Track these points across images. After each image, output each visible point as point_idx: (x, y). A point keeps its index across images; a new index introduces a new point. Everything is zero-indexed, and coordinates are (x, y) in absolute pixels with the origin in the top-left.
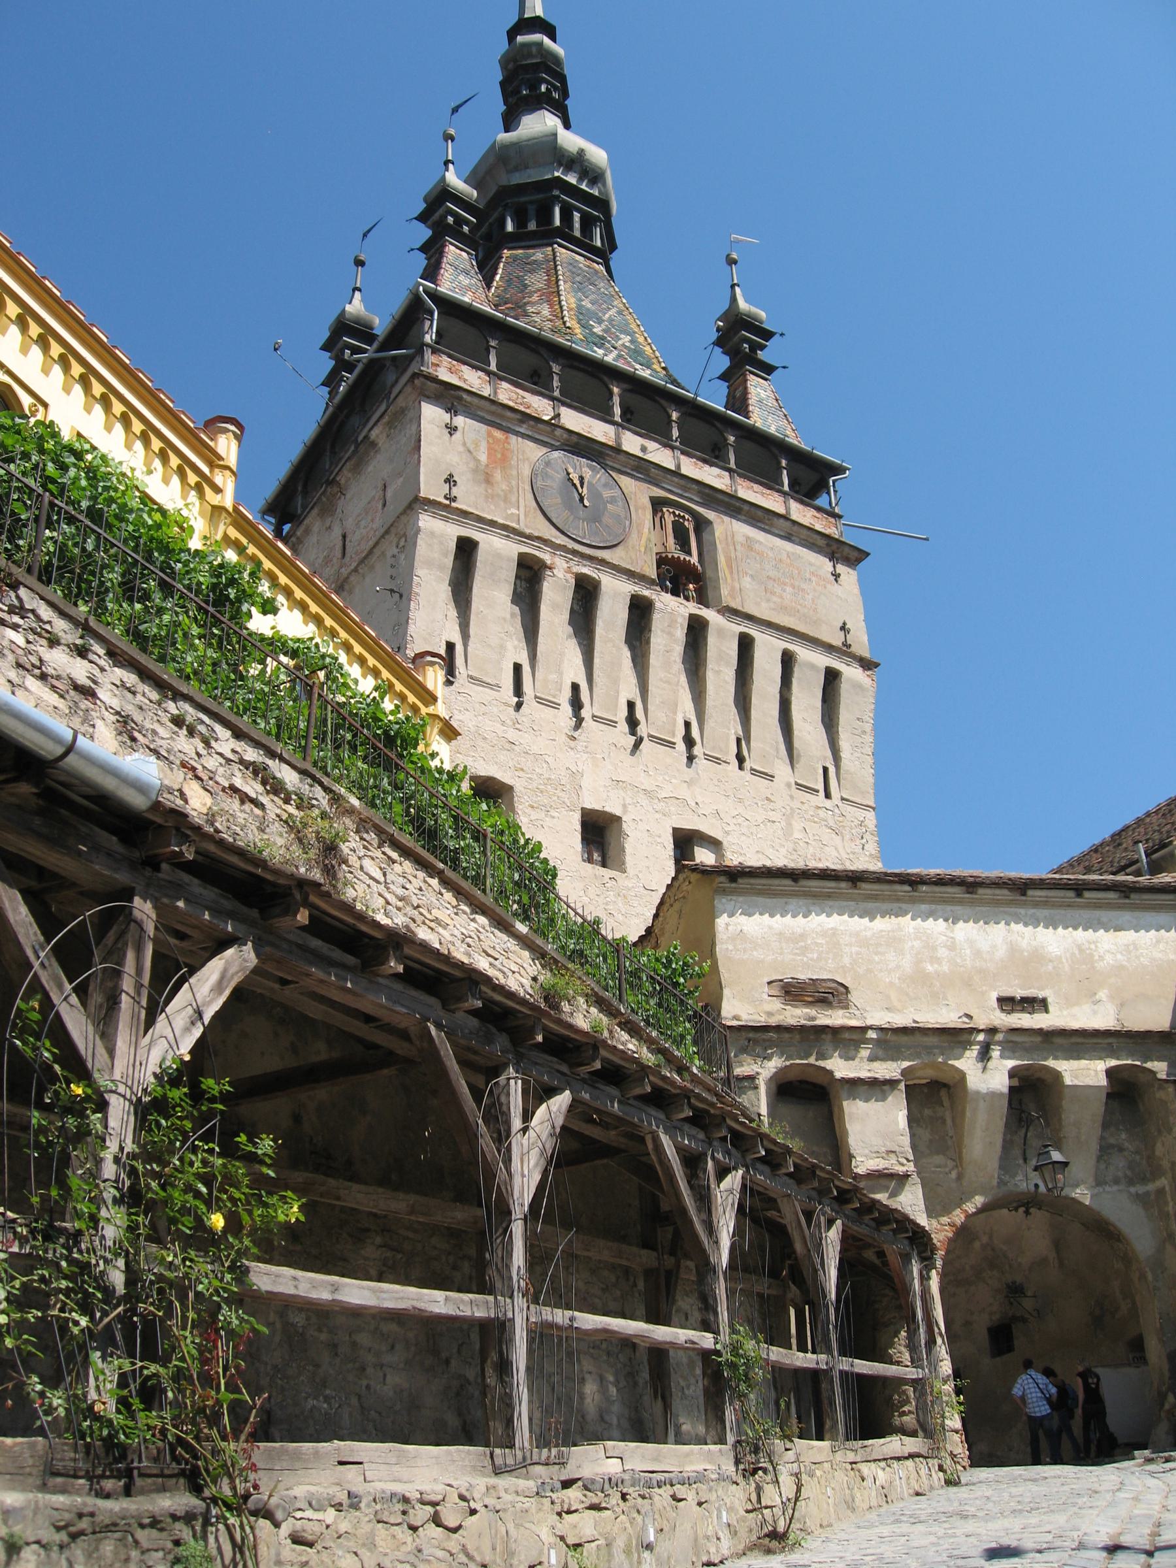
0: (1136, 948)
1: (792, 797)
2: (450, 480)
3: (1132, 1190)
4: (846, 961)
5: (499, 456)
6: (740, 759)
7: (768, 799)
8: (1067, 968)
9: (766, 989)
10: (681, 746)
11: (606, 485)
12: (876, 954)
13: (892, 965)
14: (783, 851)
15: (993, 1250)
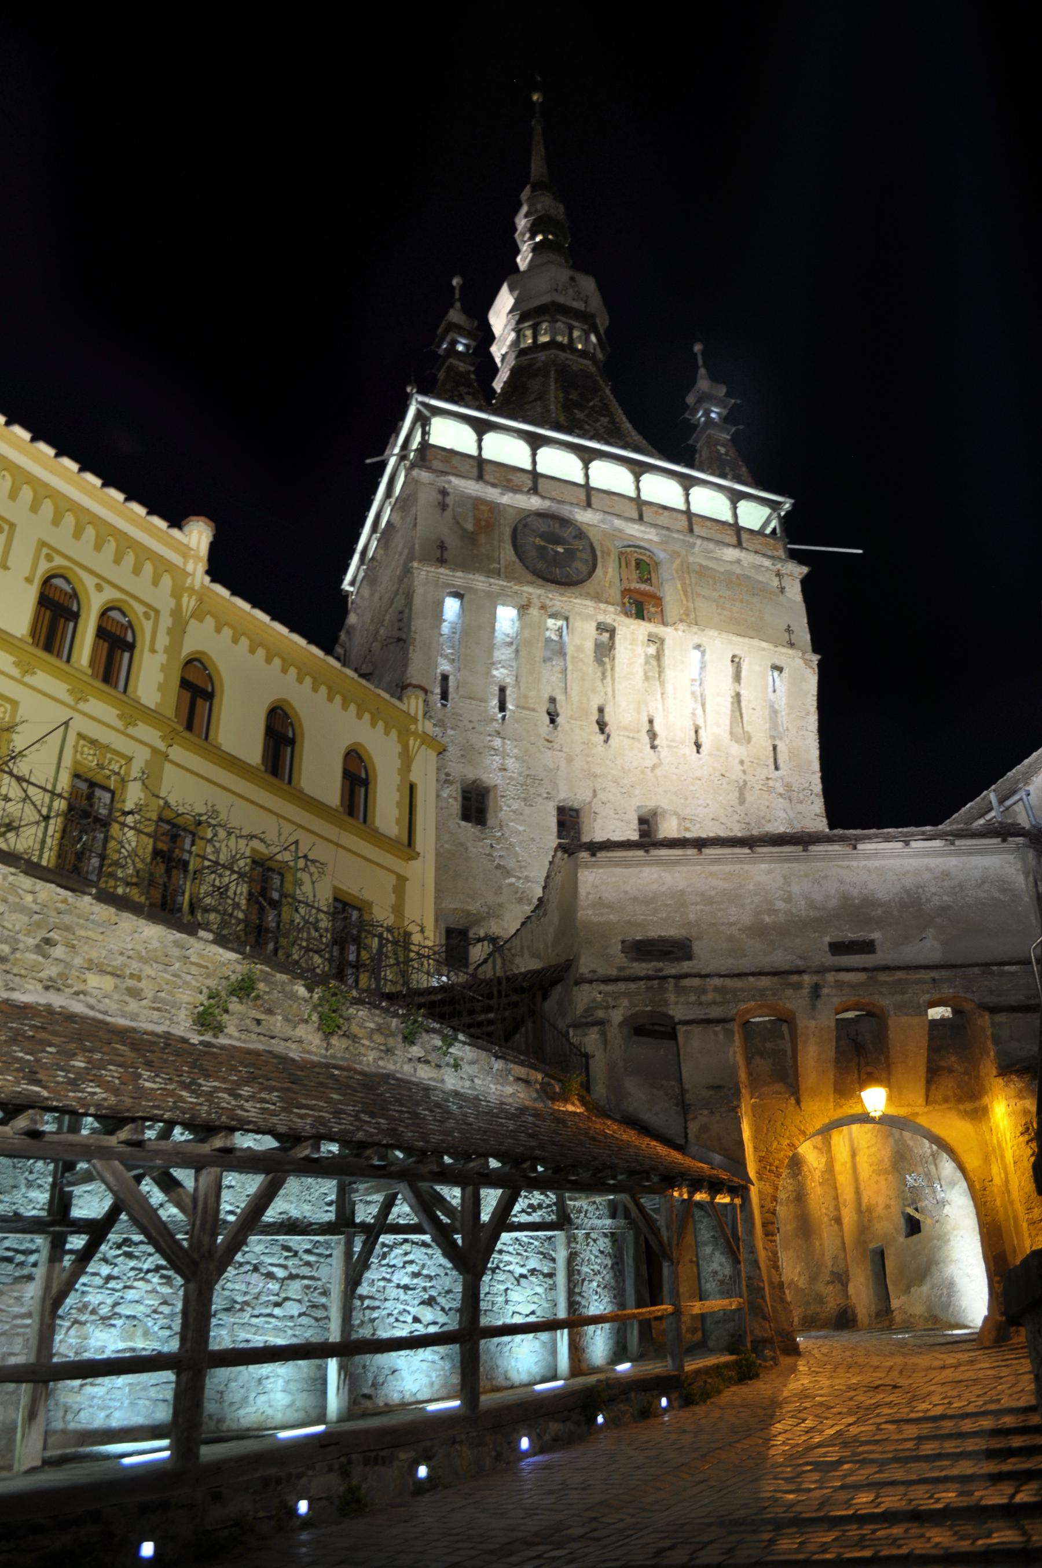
0: (962, 890)
1: (744, 772)
2: (442, 547)
3: (961, 1107)
4: (692, 917)
5: (483, 523)
6: (698, 746)
7: (723, 775)
8: (895, 913)
9: (620, 947)
10: (646, 739)
11: (575, 537)
12: (720, 910)
13: (733, 919)
14: (737, 817)
15: (903, 1144)
